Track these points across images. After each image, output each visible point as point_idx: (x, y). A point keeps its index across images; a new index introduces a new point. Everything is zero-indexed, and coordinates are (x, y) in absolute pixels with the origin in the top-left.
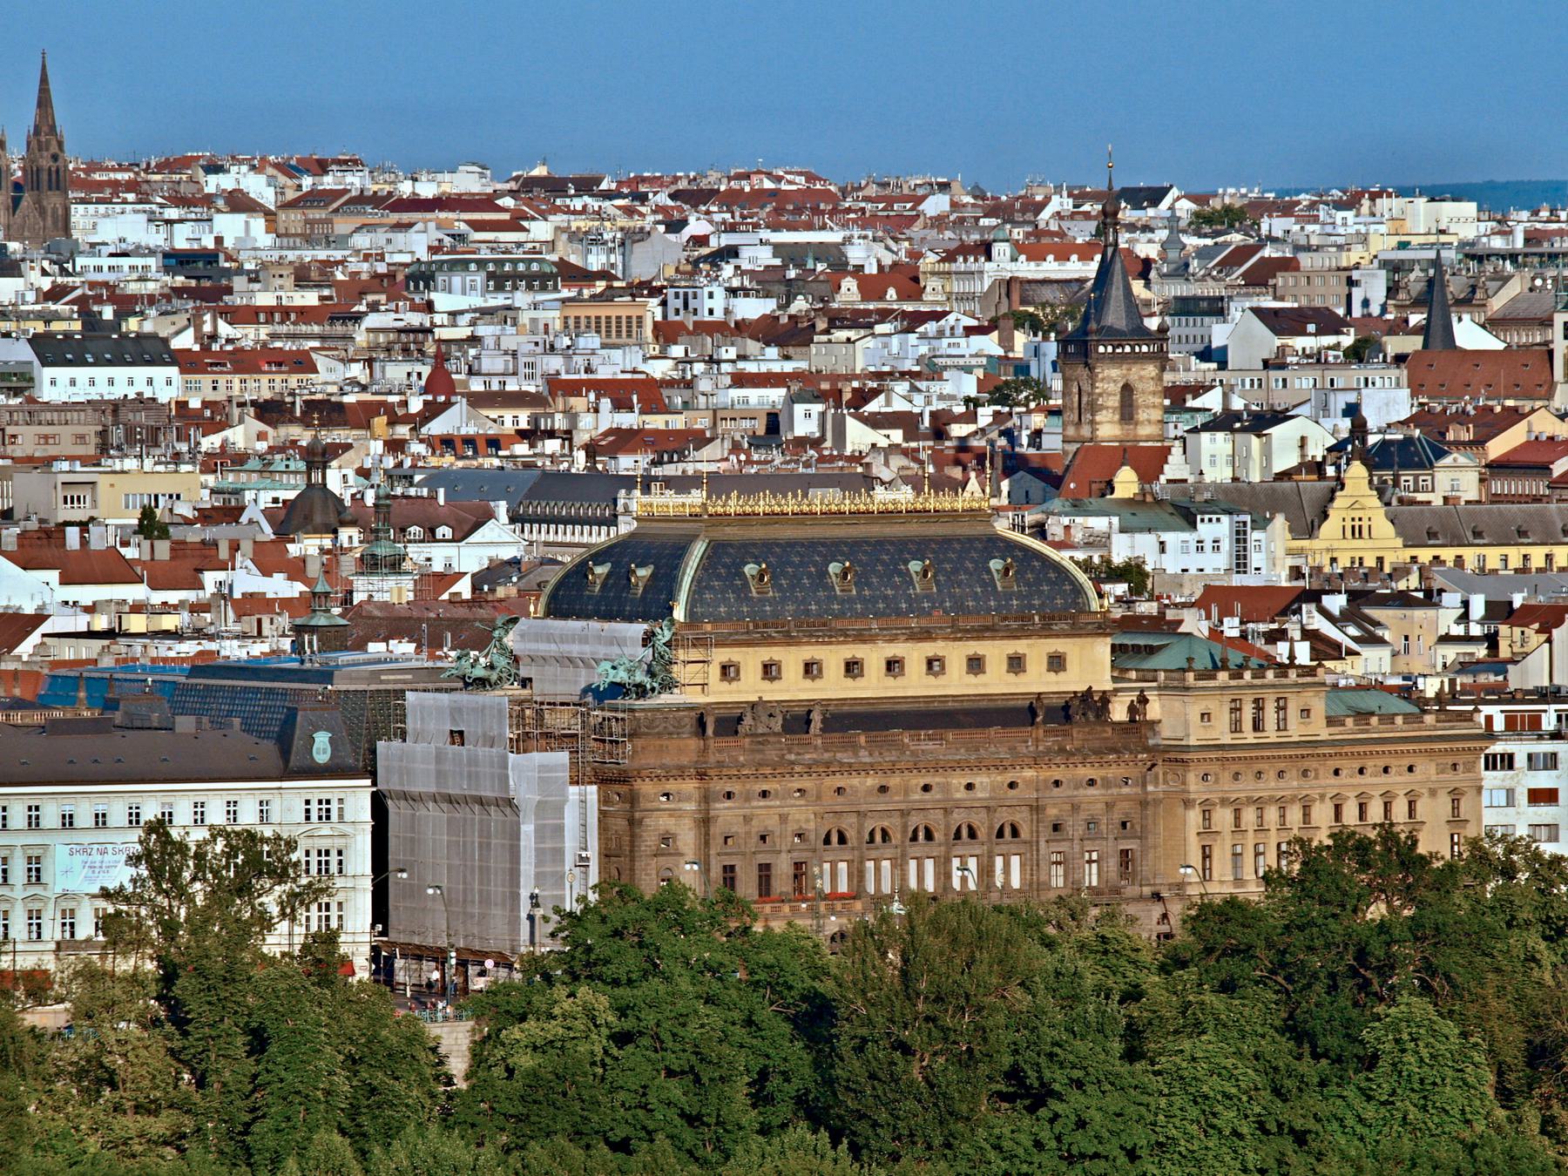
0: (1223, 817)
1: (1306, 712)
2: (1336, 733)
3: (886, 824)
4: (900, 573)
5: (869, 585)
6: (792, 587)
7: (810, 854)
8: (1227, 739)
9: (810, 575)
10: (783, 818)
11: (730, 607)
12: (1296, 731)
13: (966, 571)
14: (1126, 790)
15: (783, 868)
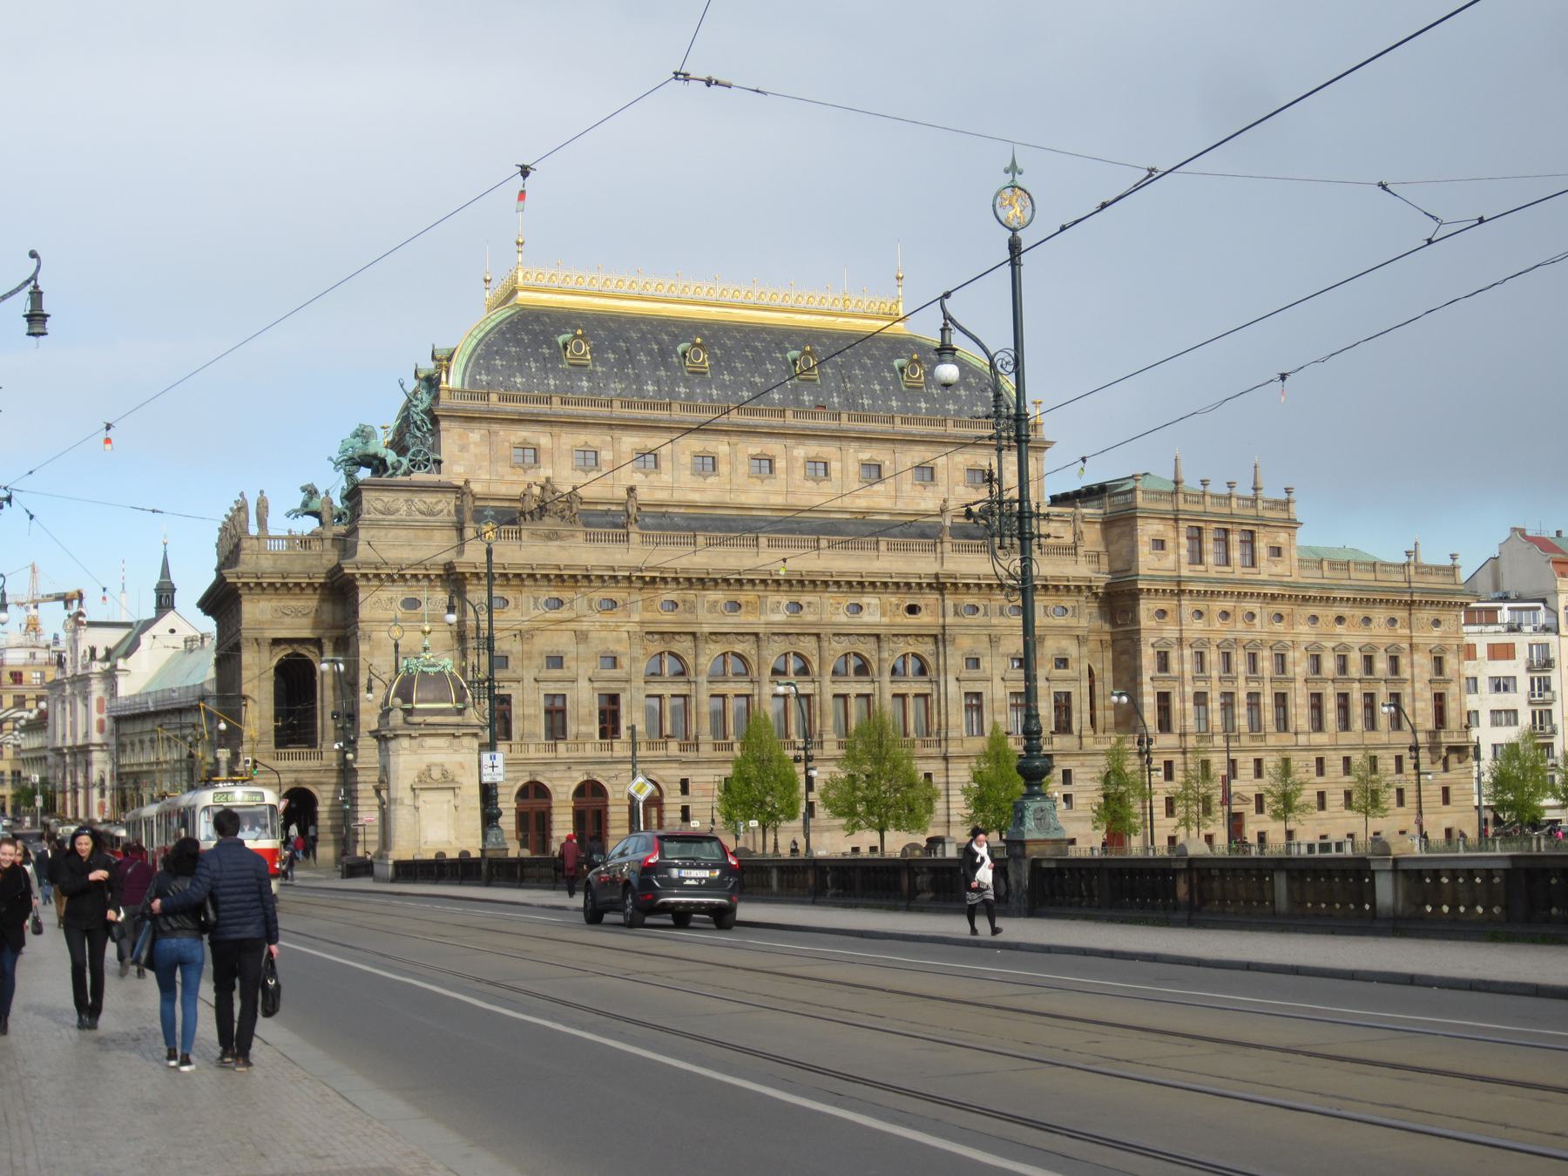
0: (1184, 663)
1: (1277, 551)
2: (1311, 576)
3: (738, 648)
4: (773, 361)
5: (732, 371)
6: (621, 364)
7: (623, 685)
8: (1185, 572)
9: (650, 353)
10: (582, 637)
11: (530, 376)
12: (1267, 568)
13: (863, 367)
14: (1061, 621)
15: (584, 703)
